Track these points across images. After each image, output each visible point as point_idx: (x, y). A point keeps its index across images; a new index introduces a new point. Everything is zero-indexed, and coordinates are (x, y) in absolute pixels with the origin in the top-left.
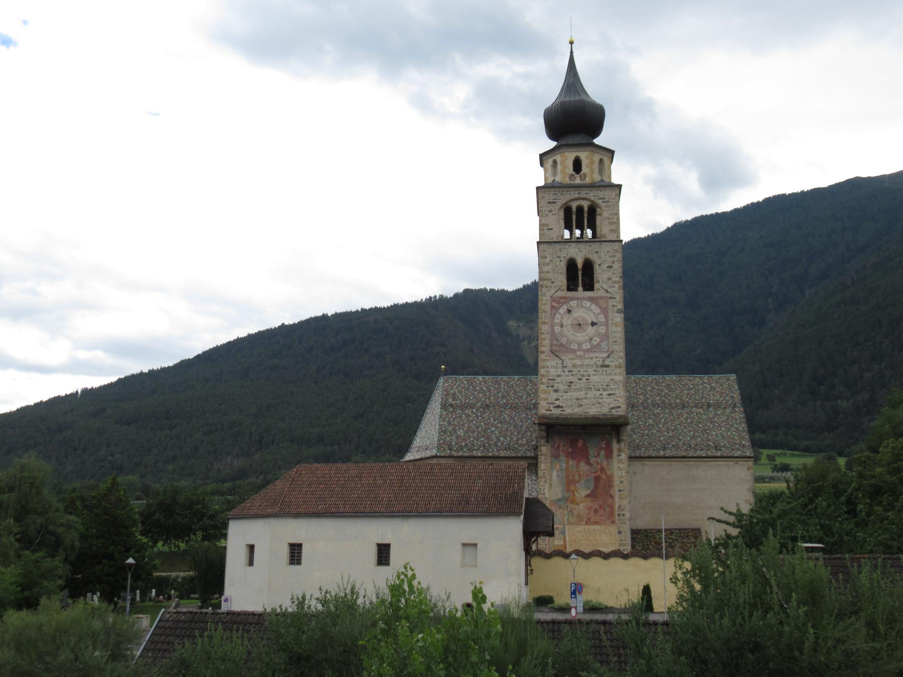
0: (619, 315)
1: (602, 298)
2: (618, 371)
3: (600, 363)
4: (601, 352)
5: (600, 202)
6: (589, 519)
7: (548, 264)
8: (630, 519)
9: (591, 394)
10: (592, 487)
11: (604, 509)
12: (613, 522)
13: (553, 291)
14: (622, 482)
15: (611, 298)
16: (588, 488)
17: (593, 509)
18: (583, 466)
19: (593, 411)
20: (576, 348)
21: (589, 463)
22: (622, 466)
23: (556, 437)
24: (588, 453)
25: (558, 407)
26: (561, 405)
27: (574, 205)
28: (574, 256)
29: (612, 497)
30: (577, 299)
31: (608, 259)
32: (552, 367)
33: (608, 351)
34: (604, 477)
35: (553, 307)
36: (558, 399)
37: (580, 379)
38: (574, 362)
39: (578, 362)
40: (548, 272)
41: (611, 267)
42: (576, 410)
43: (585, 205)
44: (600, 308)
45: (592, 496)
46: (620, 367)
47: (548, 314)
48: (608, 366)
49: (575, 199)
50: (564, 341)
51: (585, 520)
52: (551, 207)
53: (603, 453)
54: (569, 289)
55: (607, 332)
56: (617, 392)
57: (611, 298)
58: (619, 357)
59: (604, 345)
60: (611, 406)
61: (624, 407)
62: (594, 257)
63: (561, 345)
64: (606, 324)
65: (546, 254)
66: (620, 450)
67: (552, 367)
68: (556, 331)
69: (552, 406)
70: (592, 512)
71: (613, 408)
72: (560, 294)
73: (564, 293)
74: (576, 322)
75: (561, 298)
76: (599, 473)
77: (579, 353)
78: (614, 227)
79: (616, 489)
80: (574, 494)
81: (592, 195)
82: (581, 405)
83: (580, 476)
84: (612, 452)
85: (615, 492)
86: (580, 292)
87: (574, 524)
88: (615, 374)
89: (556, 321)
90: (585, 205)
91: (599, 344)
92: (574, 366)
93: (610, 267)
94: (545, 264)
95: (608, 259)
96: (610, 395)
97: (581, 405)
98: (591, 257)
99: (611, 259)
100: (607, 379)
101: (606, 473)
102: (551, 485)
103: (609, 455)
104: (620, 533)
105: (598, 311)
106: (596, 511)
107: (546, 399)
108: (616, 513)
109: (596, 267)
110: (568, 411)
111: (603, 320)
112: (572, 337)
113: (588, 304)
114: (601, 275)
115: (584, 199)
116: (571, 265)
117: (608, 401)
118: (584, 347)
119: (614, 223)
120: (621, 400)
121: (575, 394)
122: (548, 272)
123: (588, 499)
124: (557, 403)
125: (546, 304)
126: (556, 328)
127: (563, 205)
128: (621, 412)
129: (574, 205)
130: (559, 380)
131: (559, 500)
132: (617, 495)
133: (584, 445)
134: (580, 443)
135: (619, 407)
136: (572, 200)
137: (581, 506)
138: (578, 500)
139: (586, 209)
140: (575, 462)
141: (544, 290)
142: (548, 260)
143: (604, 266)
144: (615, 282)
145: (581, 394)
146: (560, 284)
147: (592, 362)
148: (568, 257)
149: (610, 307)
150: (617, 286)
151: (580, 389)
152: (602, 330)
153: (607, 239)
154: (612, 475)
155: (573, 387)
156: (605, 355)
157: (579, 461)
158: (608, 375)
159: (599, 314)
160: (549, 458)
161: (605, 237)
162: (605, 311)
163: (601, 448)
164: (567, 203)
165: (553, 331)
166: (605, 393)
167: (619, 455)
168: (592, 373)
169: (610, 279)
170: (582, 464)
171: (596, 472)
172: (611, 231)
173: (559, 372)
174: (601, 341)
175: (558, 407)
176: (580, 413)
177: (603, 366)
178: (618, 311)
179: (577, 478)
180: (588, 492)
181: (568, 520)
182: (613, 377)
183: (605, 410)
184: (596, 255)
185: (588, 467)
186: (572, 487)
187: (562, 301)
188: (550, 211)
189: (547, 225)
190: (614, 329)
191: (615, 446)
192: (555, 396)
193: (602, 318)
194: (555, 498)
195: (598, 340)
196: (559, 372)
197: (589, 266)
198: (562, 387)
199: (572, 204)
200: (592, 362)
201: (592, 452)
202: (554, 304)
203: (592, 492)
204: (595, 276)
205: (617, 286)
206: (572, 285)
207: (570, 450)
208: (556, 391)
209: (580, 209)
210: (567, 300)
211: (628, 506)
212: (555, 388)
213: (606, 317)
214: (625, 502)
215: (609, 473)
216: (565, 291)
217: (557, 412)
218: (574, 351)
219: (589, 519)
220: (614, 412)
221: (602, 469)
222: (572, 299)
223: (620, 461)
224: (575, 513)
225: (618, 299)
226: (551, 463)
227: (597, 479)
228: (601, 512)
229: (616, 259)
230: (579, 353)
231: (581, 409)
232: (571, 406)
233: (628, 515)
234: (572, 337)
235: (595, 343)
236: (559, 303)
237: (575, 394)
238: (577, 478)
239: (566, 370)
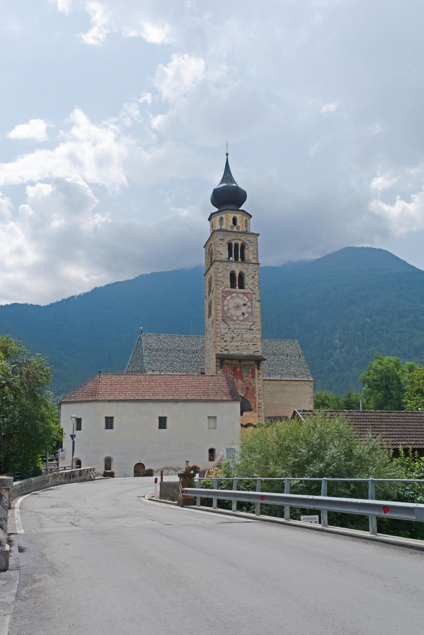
0: (258, 303)
1: (249, 293)
2: (257, 332)
3: (248, 328)
4: (249, 322)
5: (248, 242)
7: (220, 273)
8: (264, 409)
9: (244, 344)
10: (245, 392)
13: (223, 288)
14: (260, 390)
15: (254, 294)
18: (240, 382)
19: (245, 353)
20: (236, 319)
21: (243, 380)
22: (260, 382)
23: (225, 366)
24: (242, 375)
25: (226, 350)
26: (228, 349)
27: (234, 243)
28: (234, 270)
29: (255, 398)
30: (236, 293)
31: (252, 273)
32: (223, 328)
33: (252, 321)
34: (250, 387)
35: (223, 296)
36: (226, 346)
37: (238, 336)
38: (235, 326)
39: (237, 327)
40: (220, 277)
41: (254, 277)
42: (236, 352)
43: (240, 243)
44: (248, 298)
46: (259, 330)
47: (221, 300)
48: (253, 330)
49: (235, 239)
50: (229, 315)
52: (221, 242)
53: (250, 375)
54: (231, 288)
55: (252, 312)
56: (257, 343)
57: (254, 294)
58: (258, 326)
59: (250, 317)
60: (254, 350)
61: (261, 351)
62: (245, 271)
63: (228, 317)
64: (251, 307)
65: (219, 267)
66: (259, 374)
67: (223, 328)
68: (225, 309)
69: (223, 349)
71: (255, 352)
72: (227, 289)
73: (229, 289)
74: (236, 305)
75: (227, 291)
76: (248, 385)
77: (237, 322)
78: (255, 256)
79: (257, 394)
81: (244, 238)
82: (238, 350)
84: (255, 375)
85: (256, 395)
86: (237, 289)
88: (257, 334)
89: (225, 304)
90: (240, 243)
91: (248, 318)
92: (235, 328)
93: (254, 277)
94: (218, 273)
95: (252, 273)
96: (253, 345)
97: (238, 350)
98: (243, 271)
99: (254, 273)
100: (252, 336)
103: (253, 376)
104: (259, 416)
105: (247, 300)
107: (220, 345)
108: (257, 406)
109: (246, 276)
110: (232, 352)
111: (250, 305)
112: (234, 313)
113: (242, 296)
114: (248, 281)
115: (239, 240)
116: (232, 275)
117: (252, 348)
118: (240, 319)
119: (255, 254)
120: (259, 348)
121: (235, 344)
122: (220, 277)
124: (226, 348)
125: (219, 294)
126: (225, 307)
127: (228, 241)
128: (259, 354)
129: (234, 243)
130: (226, 335)
132: (257, 397)
133: (240, 370)
134: (238, 370)
135: (258, 351)
136: (232, 240)
139: (240, 245)
141: (218, 286)
142: (220, 271)
143: (250, 277)
144: (256, 285)
145: (239, 344)
146: (227, 284)
147: (244, 327)
148: (231, 270)
149: (254, 298)
150: (257, 287)
151: (238, 341)
152: (250, 310)
153: (252, 262)
154: (255, 387)
155: (234, 339)
156: (251, 324)
157: (238, 379)
158: (252, 334)
159: (248, 302)
161: (251, 261)
162: (251, 300)
163: (249, 373)
164: (230, 241)
165: (223, 309)
166: (251, 344)
168: (244, 332)
169: (253, 283)
170: (240, 380)
171: (247, 385)
172: (254, 258)
173: (227, 331)
174: (249, 316)
175: (226, 350)
176: (238, 353)
177: (250, 329)
178: (258, 301)
182: (254, 336)
183: (251, 353)
184: (246, 270)
185: (243, 382)
187: (228, 293)
188: (221, 244)
189: (220, 252)
190: (255, 310)
191: (256, 371)
192: (225, 344)
193: (249, 304)
195: (248, 315)
196: (227, 331)
197: (241, 276)
198: (228, 340)
199: (232, 241)
200: (244, 327)
201: (244, 374)
202: (224, 294)
204: (245, 281)
205: (257, 287)
206: (233, 286)
207: (233, 373)
208: (225, 341)
209: (236, 245)
210: (231, 293)
211: (263, 403)
212: (225, 340)
213: (252, 303)
214: (262, 401)
215: (253, 385)
216: (230, 288)
217: (226, 352)
218: (235, 321)
220: (256, 354)
221: (250, 383)
222: (233, 293)
223: (259, 380)
225: (258, 294)
227: (247, 388)
229: (256, 273)
230: (237, 322)
231: (239, 351)
232: (233, 350)
233: (263, 407)
234: (234, 313)
235: (245, 317)
236: (226, 294)
237: (235, 344)
239: (231, 330)
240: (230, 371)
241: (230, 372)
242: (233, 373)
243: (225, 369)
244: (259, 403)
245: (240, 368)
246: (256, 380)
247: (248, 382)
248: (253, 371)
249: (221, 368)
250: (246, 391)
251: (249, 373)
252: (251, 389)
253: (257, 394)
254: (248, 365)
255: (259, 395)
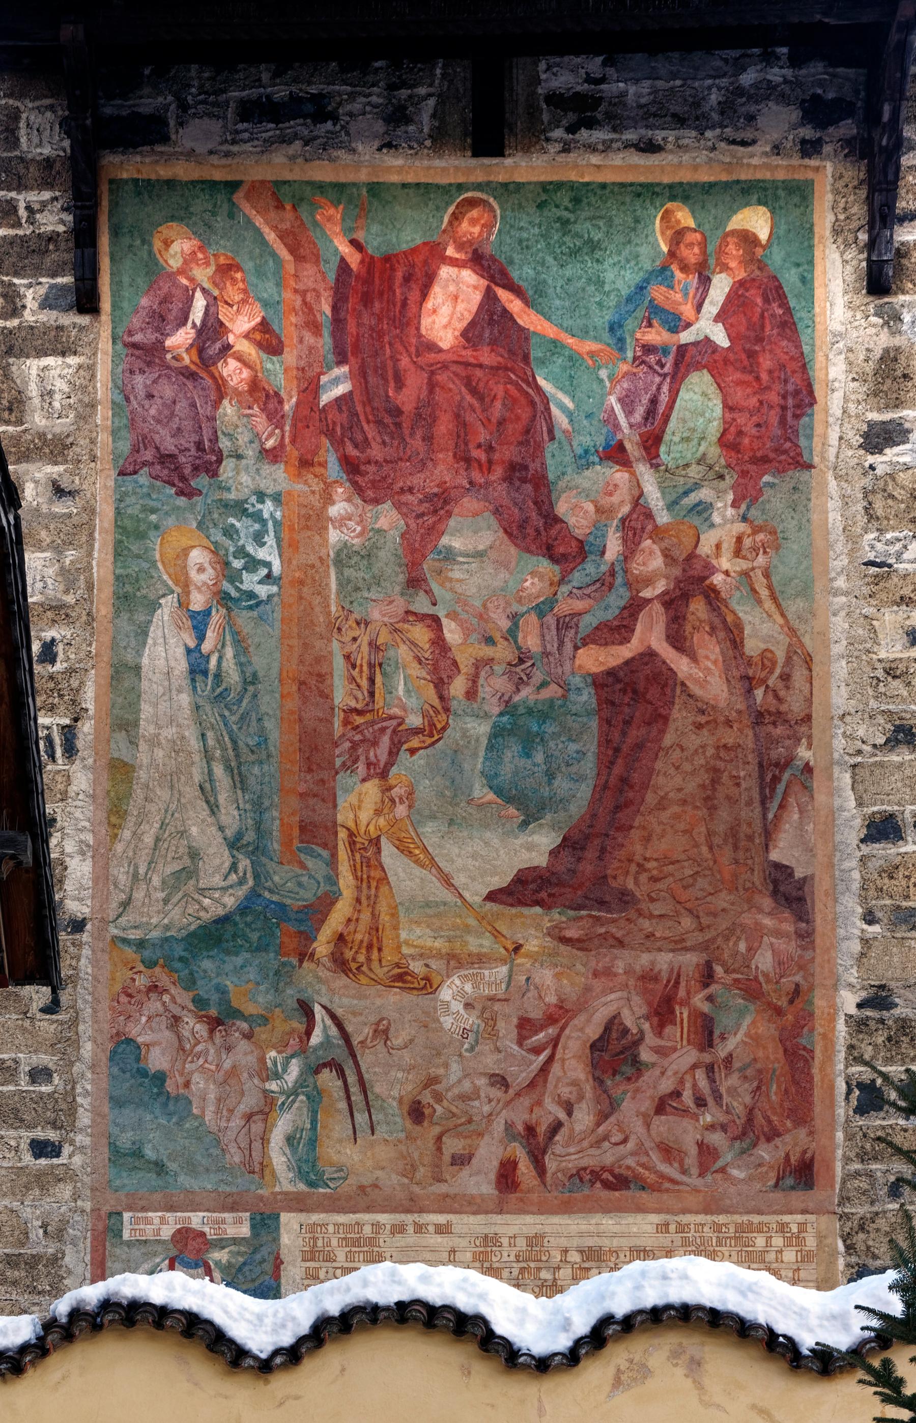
6: (537, 1141)
10: (578, 794)
11: (706, 1033)
12: (803, 1173)
16: (529, 808)
17: (589, 1027)
21: (538, 529)
23: (177, 248)
24: (531, 419)
29: (791, 894)
34: (703, 673)
45: (575, 885)
51: (489, 1153)
70: (572, 1067)
76: (650, 633)
80: (371, 875)
83: (440, 664)
84: (802, 398)
87: (365, 1198)
101: (733, 636)
102: (120, 771)
106: (614, 1055)
108: (838, 1073)
123: (532, 928)
131: (214, 936)
133: (491, 323)
134: (448, 307)
137: (451, 991)
138: (414, 937)
140: (387, 518)
157: (440, 504)
160: (100, 486)
167: (880, 437)
171: (618, 630)
179: (406, 693)
180: (537, 847)
181: (306, 1148)
185: (534, 576)
186: (358, 802)
194: (161, 915)
203: (571, 844)
215: (760, 630)
219: (537, 1141)
224: (391, 1083)
226: (130, 534)
228: (673, 1061)
238: (406, 693)
240: (268, 339)
241: (278, 372)
242: (337, 385)
243: (166, 317)
244: (878, 999)
245: (478, 260)
246: (833, 503)
247: (651, 560)
248: (769, 315)
249: (86, 301)
250: (610, 751)
251: (686, 360)
252: (707, 716)
253: (851, 829)
254: (649, 192)
255: (883, 829)
